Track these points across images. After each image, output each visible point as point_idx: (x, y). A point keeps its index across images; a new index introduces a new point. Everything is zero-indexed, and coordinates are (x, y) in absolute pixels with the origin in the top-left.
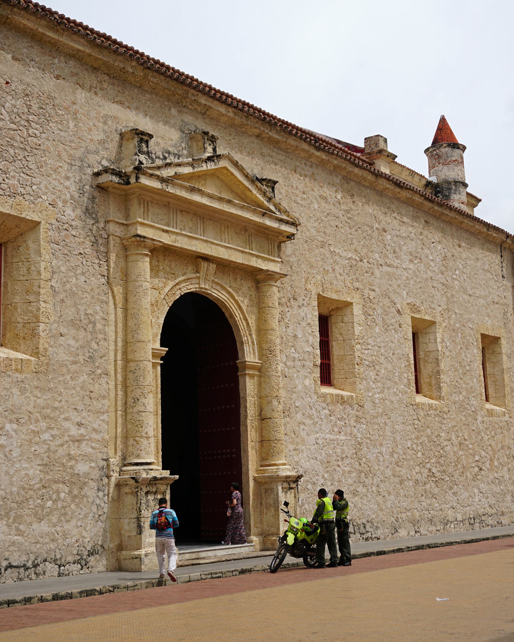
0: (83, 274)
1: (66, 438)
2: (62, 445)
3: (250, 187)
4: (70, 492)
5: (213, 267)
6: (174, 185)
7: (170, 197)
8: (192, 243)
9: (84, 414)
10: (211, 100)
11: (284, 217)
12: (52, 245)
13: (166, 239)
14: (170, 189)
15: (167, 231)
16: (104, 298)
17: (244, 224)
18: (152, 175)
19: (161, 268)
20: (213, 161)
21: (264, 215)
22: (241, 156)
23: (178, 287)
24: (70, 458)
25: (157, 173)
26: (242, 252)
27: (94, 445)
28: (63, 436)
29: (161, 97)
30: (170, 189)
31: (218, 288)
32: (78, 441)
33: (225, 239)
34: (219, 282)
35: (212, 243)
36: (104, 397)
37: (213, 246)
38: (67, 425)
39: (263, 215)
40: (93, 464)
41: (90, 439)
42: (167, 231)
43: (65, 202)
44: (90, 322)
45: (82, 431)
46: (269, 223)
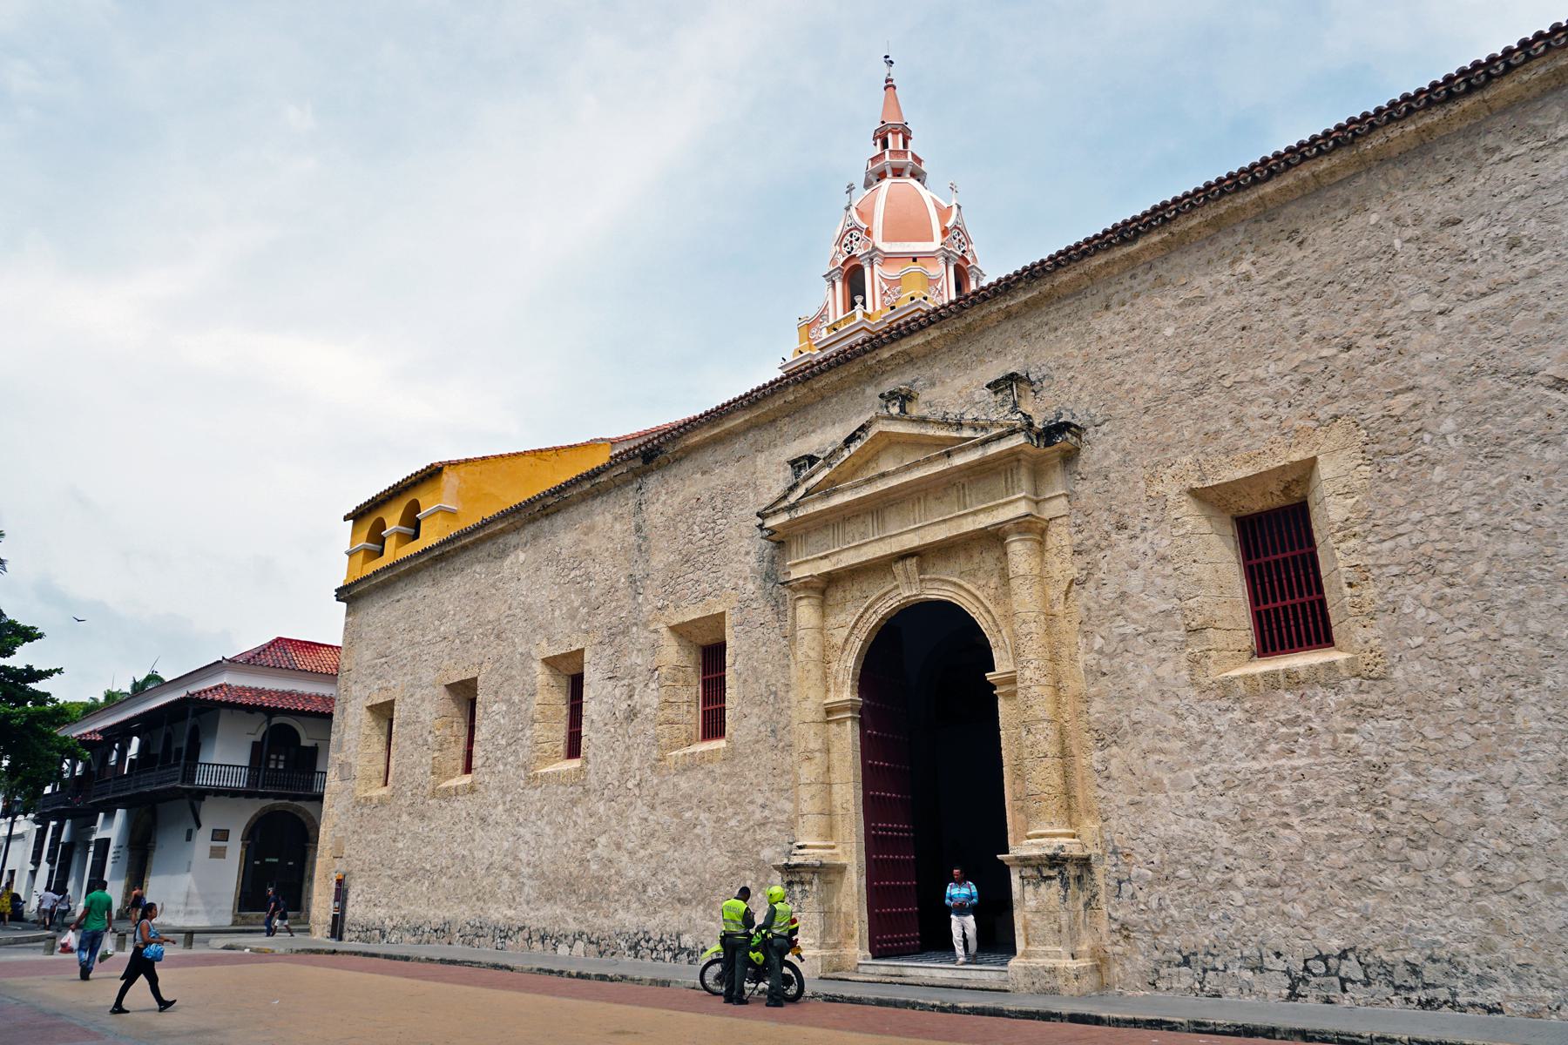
0: (764, 644)
1: (751, 823)
2: (748, 830)
3: (923, 431)
4: (757, 879)
5: (912, 564)
6: (803, 504)
7: (800, 523)
8: (862, 552)
9: (768, 794)
10: (894, 345)
11: (995, 431)
12: (736, 629)
13: (826, 567)
14: (801, 513)
15: (826, 557)
16: (786, 662)
17: (945, 480)
18: (775, 513)
19: (849, 597)
20: (859, 437)
21: (949, 455)
22: (983, 368)
23: (871, 611)
24: (757, 843)
25: (785, 504)
26: (944, 521)
27: (778, 827)
28: (749, 820)
29: (850, 388)
30: (801, 513)
31: (936, 585)
32: (764, 824)
33: (914, 519)
34: (934, 576)
35: (891, 536)
36: (788, 773)
37: (893, 539)
38: (750, 808)
39: (949, 456)
40: (778, 850)
41: (774, 822)
42: (826, 557)
43: (746, 579)
44: (771, 693)
45: (767, 813)
46: (959, 460)
